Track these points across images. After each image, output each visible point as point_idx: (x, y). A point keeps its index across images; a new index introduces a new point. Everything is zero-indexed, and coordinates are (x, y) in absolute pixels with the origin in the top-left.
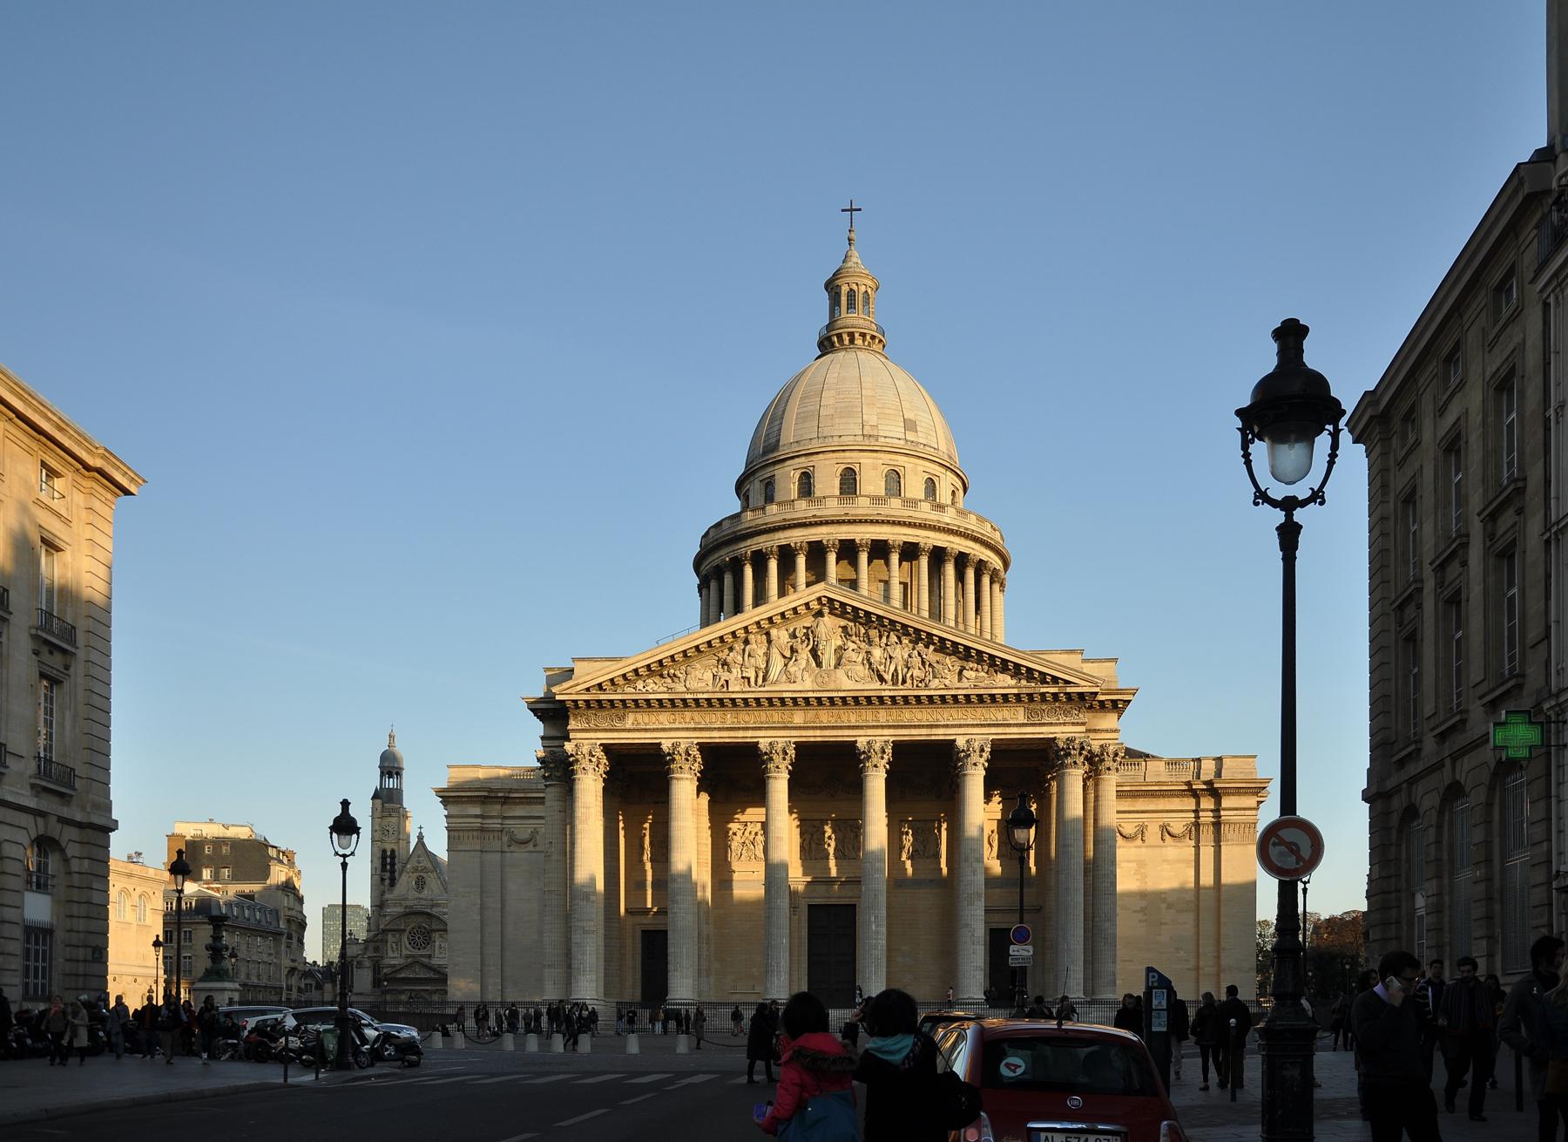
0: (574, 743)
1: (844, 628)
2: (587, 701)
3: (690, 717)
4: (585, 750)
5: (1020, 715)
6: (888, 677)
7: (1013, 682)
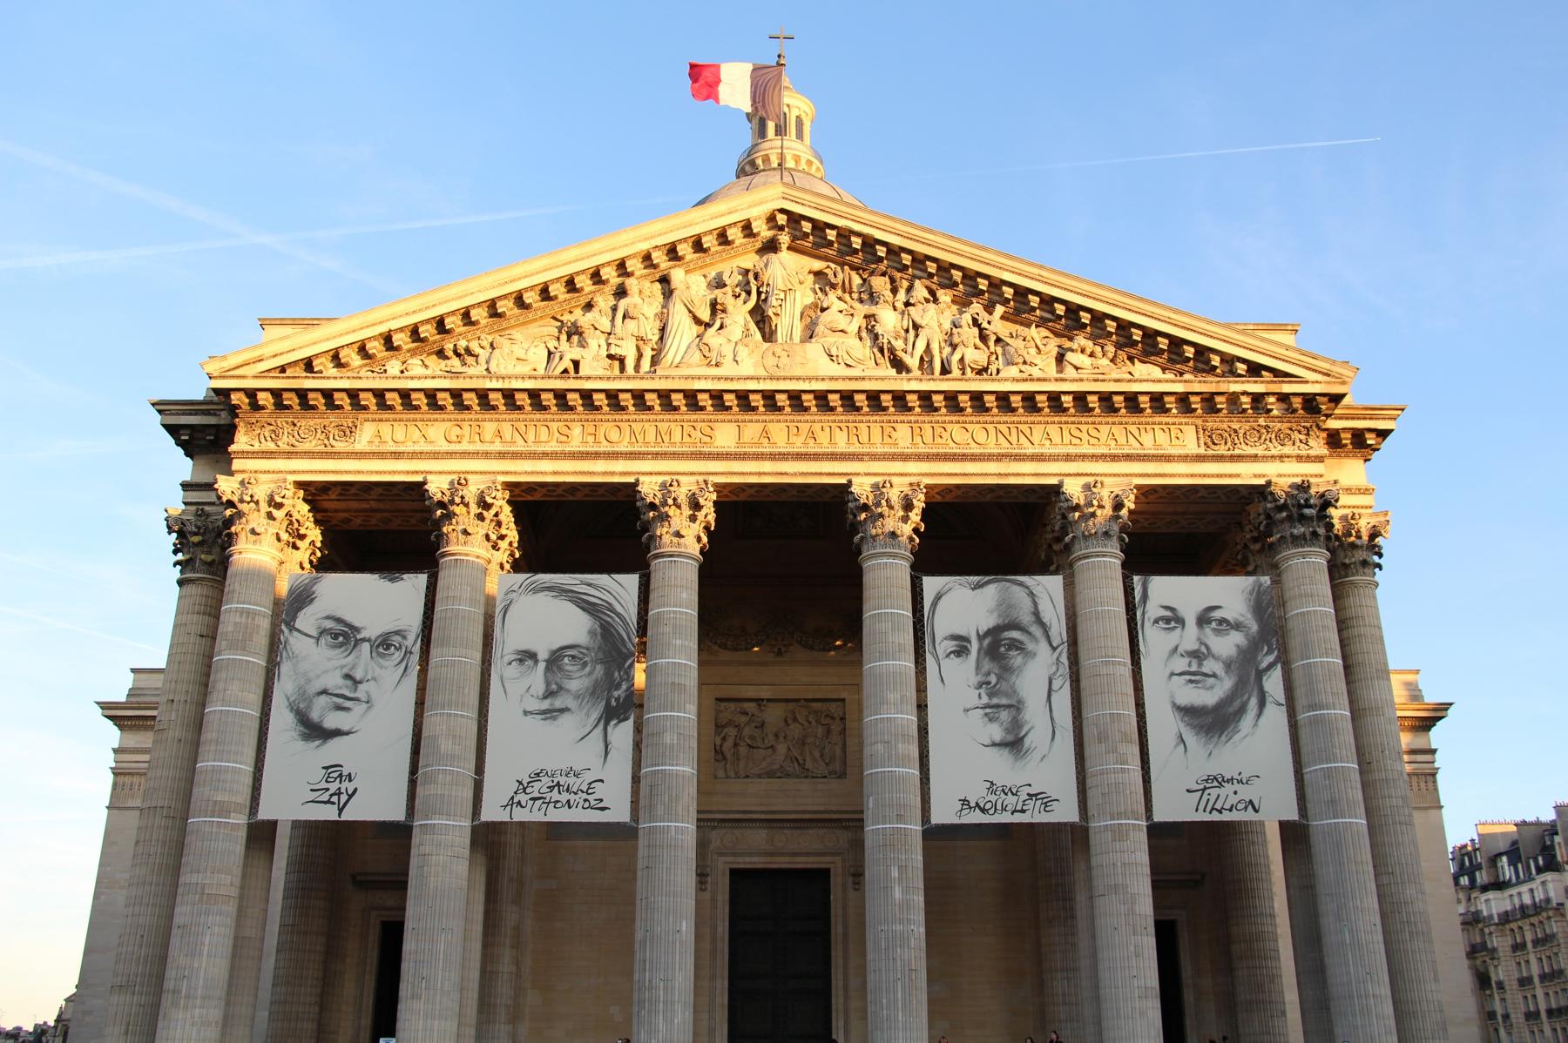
0: (239, 477)
1: (818, 274)
2: (277, 394)
3: (495, 430)
4: (261, 492)
5: (1188, 439)
6: (912, 362)
7: (1170, 376)
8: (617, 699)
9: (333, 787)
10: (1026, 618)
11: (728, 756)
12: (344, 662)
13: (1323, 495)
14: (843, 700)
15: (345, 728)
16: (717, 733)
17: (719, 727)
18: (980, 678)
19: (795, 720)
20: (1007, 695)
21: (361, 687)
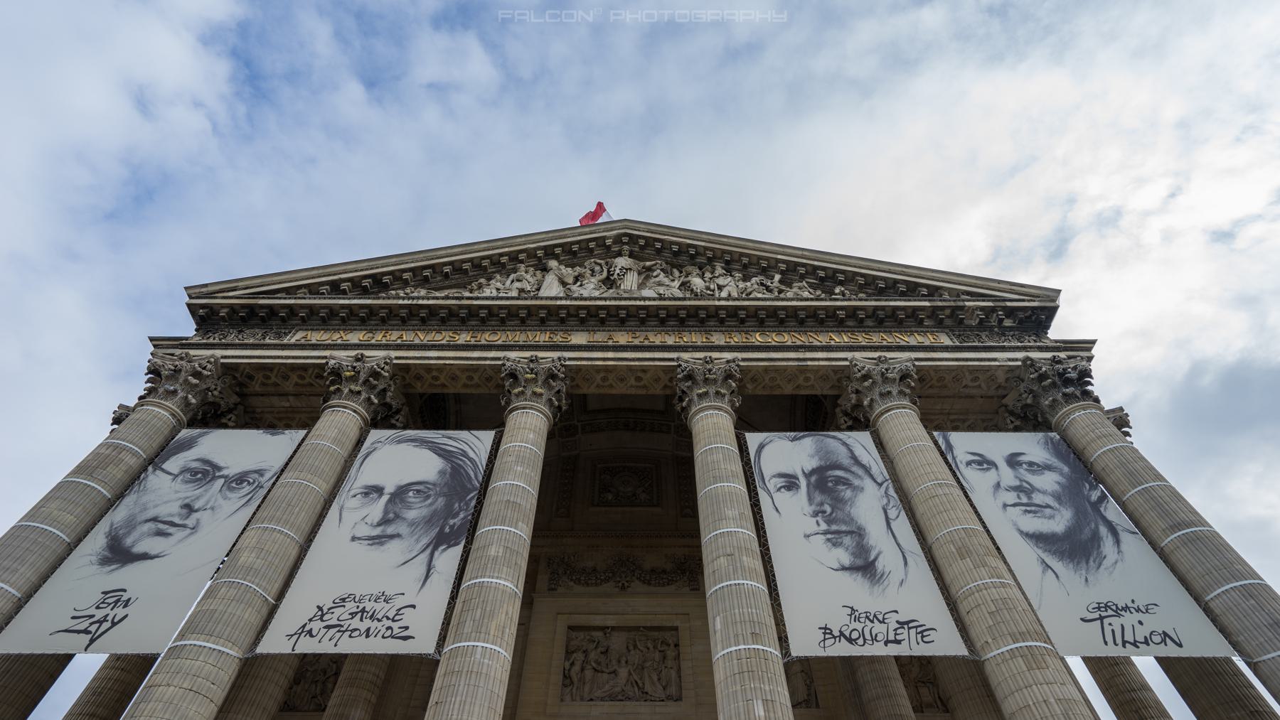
8: (452, 527)
9: (99, 614)
10: (846, 461)
11: (575, 679)
12: (189, 494)
13: (1075, 368)
14: (676, 629)
15: (153, 553)
16: (567, 658)
17: (568, 653)
18: (813, 508)
19: (635, 647)
20: (845, 523)
21: (195, 516)
